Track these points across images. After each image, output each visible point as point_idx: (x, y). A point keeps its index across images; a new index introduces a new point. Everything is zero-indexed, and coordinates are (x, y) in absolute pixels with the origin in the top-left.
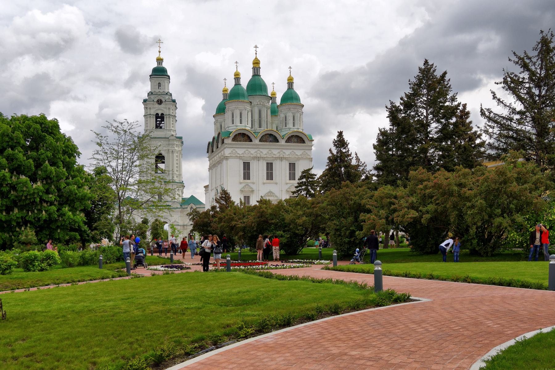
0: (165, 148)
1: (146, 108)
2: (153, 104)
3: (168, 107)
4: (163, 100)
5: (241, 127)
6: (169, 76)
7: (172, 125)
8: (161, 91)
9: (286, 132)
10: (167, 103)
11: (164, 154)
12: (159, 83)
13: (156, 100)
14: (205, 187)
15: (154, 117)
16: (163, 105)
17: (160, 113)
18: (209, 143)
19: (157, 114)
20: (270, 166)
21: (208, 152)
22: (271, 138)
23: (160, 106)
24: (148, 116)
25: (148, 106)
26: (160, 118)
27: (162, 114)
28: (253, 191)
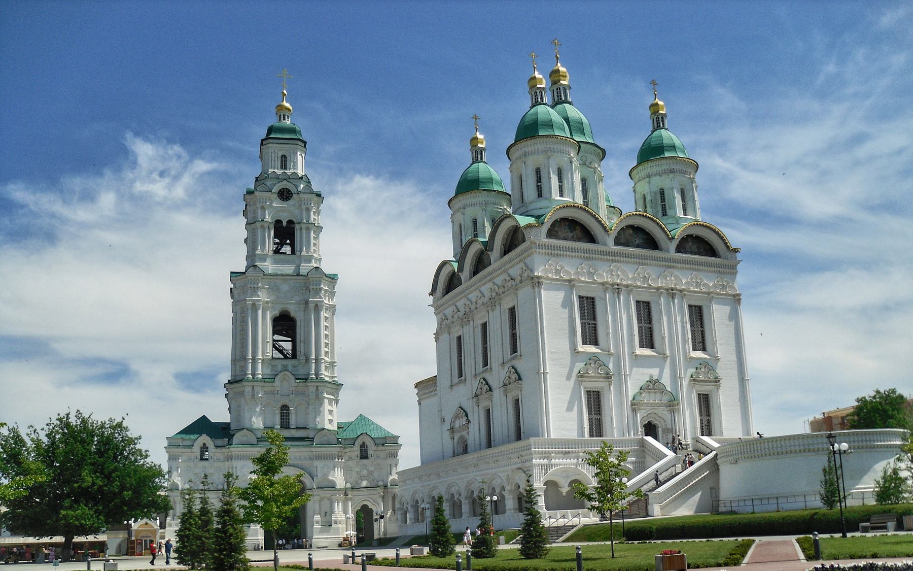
4: (293, 190)
5: (567, 199)
6: (305, 143)
7: (312, 248)
8: (289, 172)
9: (682, 221)
10: (302, 195)
13: (276, 189)
14: (417, 385)
15: (272, 226)
16: (291, 202)
18: (444, 264)
19: (278, 222)
20: (645, 311)
21: (431, 294)
22: (639, 237)
26: (286, 233)
27: (290, 222)
28: (608, 377)
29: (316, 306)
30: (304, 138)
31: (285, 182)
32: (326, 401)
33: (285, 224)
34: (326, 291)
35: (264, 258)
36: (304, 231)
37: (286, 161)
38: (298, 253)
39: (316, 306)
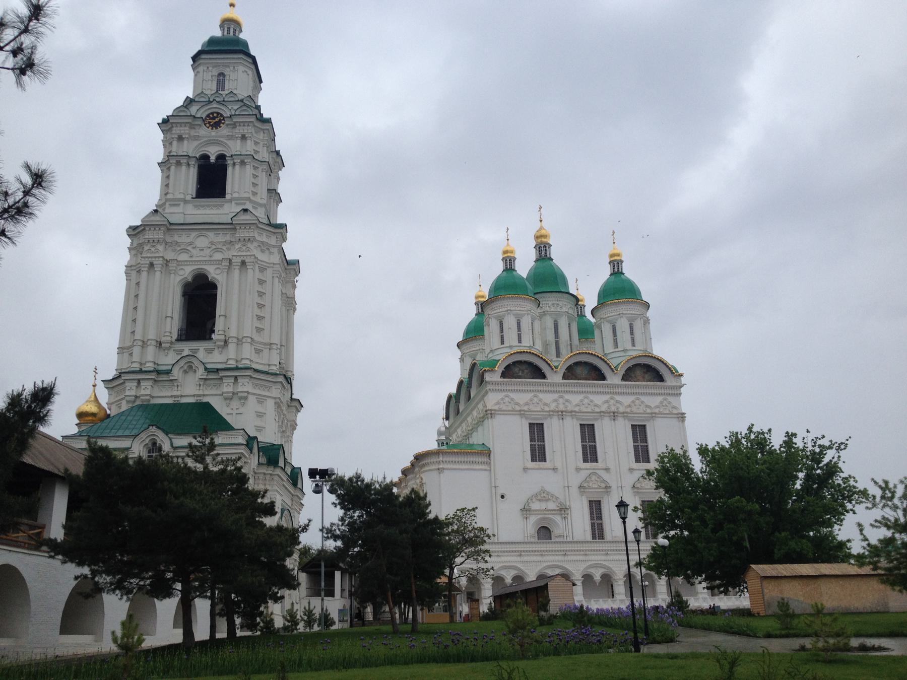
0: (218, 256)
1: (167, 143)
2: (192, 127)
3: (240, 130)
4: (226, 113)
6: (254, 59)
11: (213, 273)
12: (221, 74)
15: (192, 162)
16: (224, 131)
17: (213, 152)
19: (205, 157)
23: (213, 133)
24: (173, 161)
25: (177, 131)
27: (221, 157)
29: (243, 263)
30: (252, 53)
31: (214, 105)
32: (252, 399)
33: (213, 159)
34: (263, 243)
35: (175, 203)
36: (237, 167)
37: (224, 81)
38: (228, 197)
39: (243, 263)
